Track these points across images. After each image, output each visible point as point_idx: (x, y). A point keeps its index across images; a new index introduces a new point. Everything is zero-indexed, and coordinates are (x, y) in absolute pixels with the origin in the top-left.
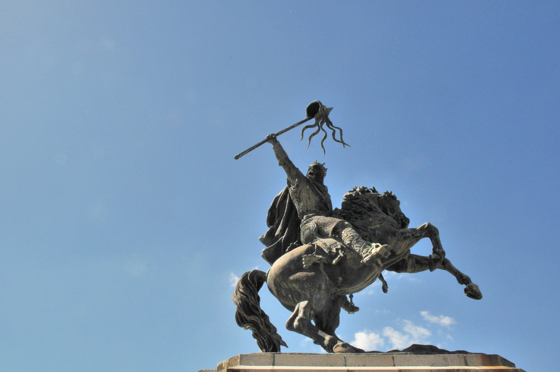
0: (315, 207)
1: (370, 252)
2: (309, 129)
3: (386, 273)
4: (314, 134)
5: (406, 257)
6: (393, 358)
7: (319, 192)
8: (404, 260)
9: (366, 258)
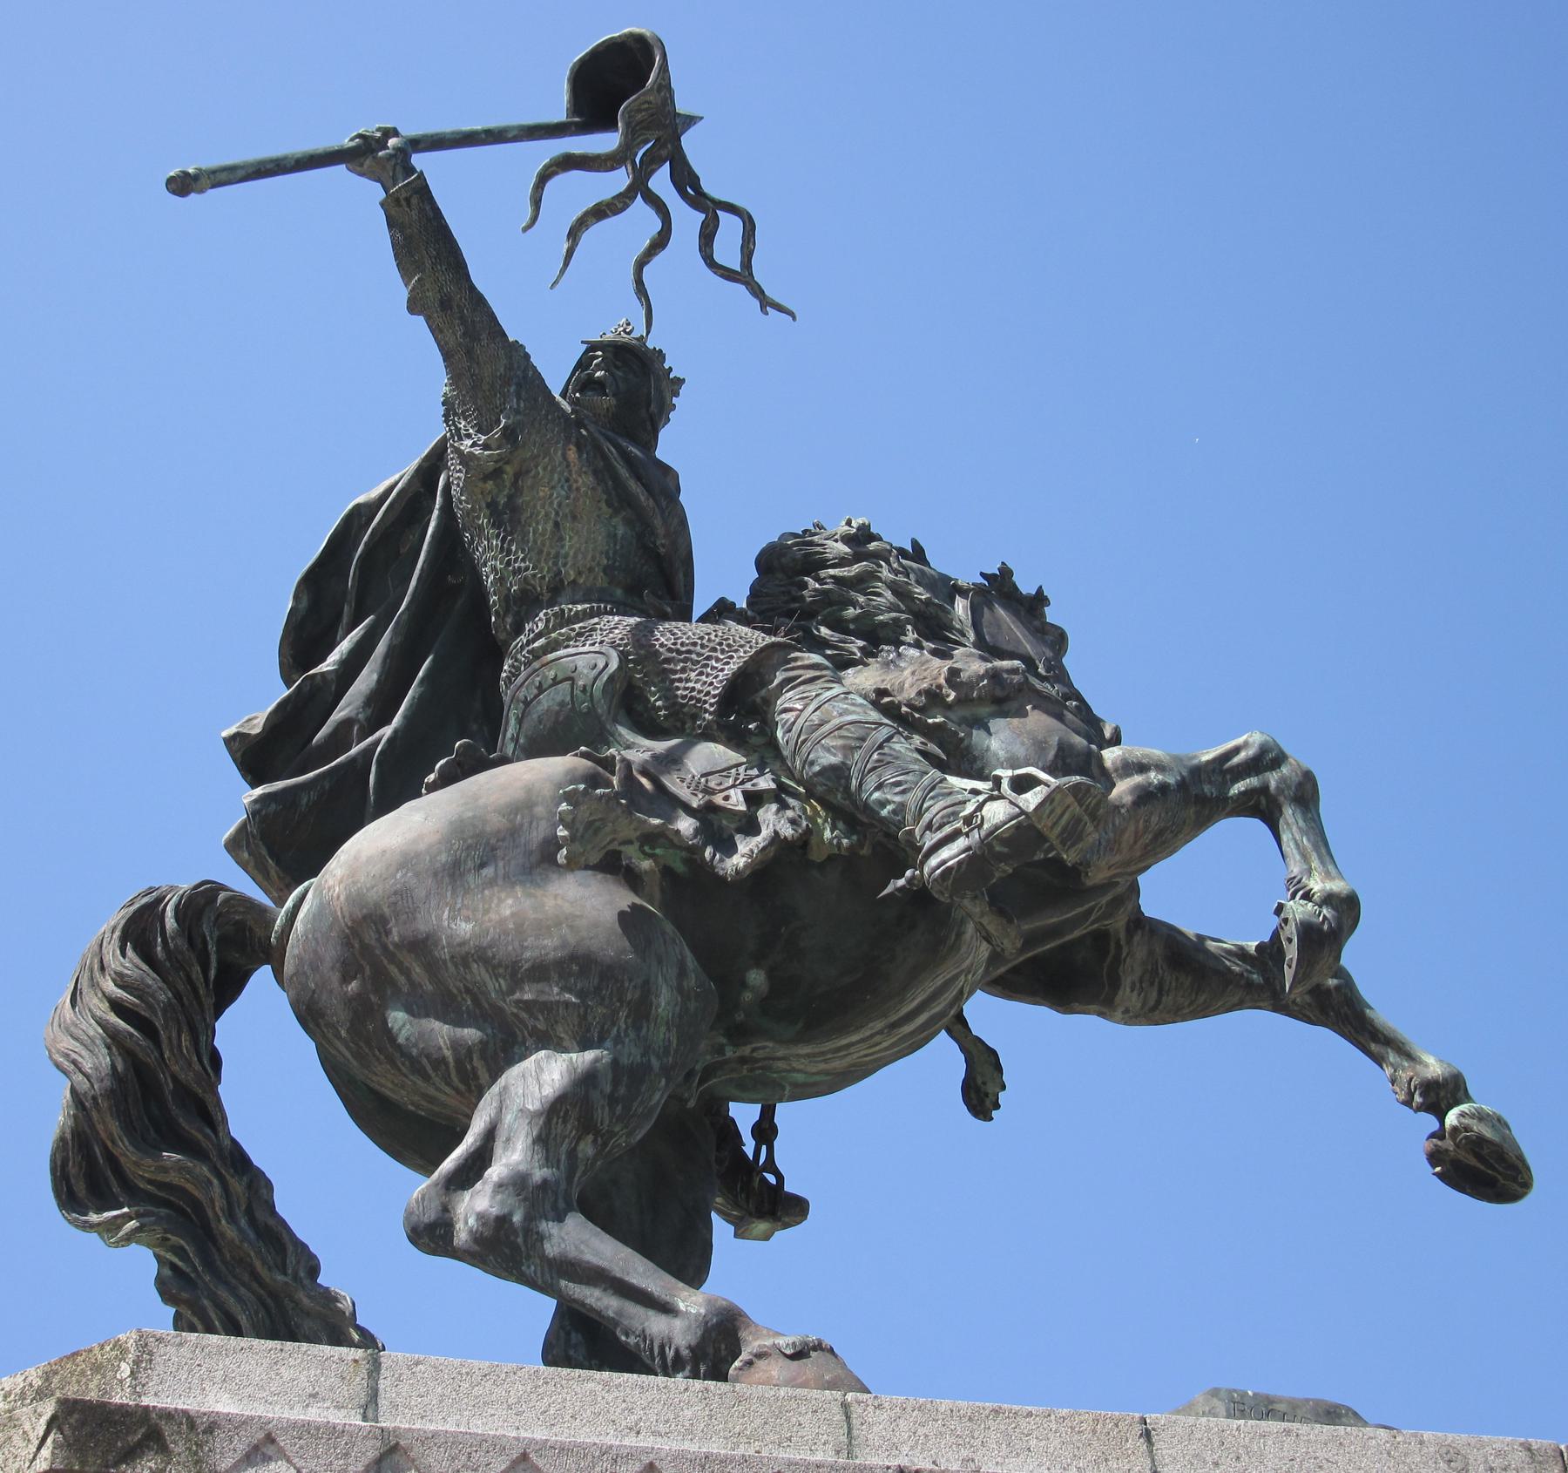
0: (607, 570)
1: (968, 821)
2: (575, 175)
3: (987, 1013)
4: (600, 212)
5: (1119, 923)
6: (1147, 1435)
7: (633, 485)
8: (1101, 939)
9: (945, 853)
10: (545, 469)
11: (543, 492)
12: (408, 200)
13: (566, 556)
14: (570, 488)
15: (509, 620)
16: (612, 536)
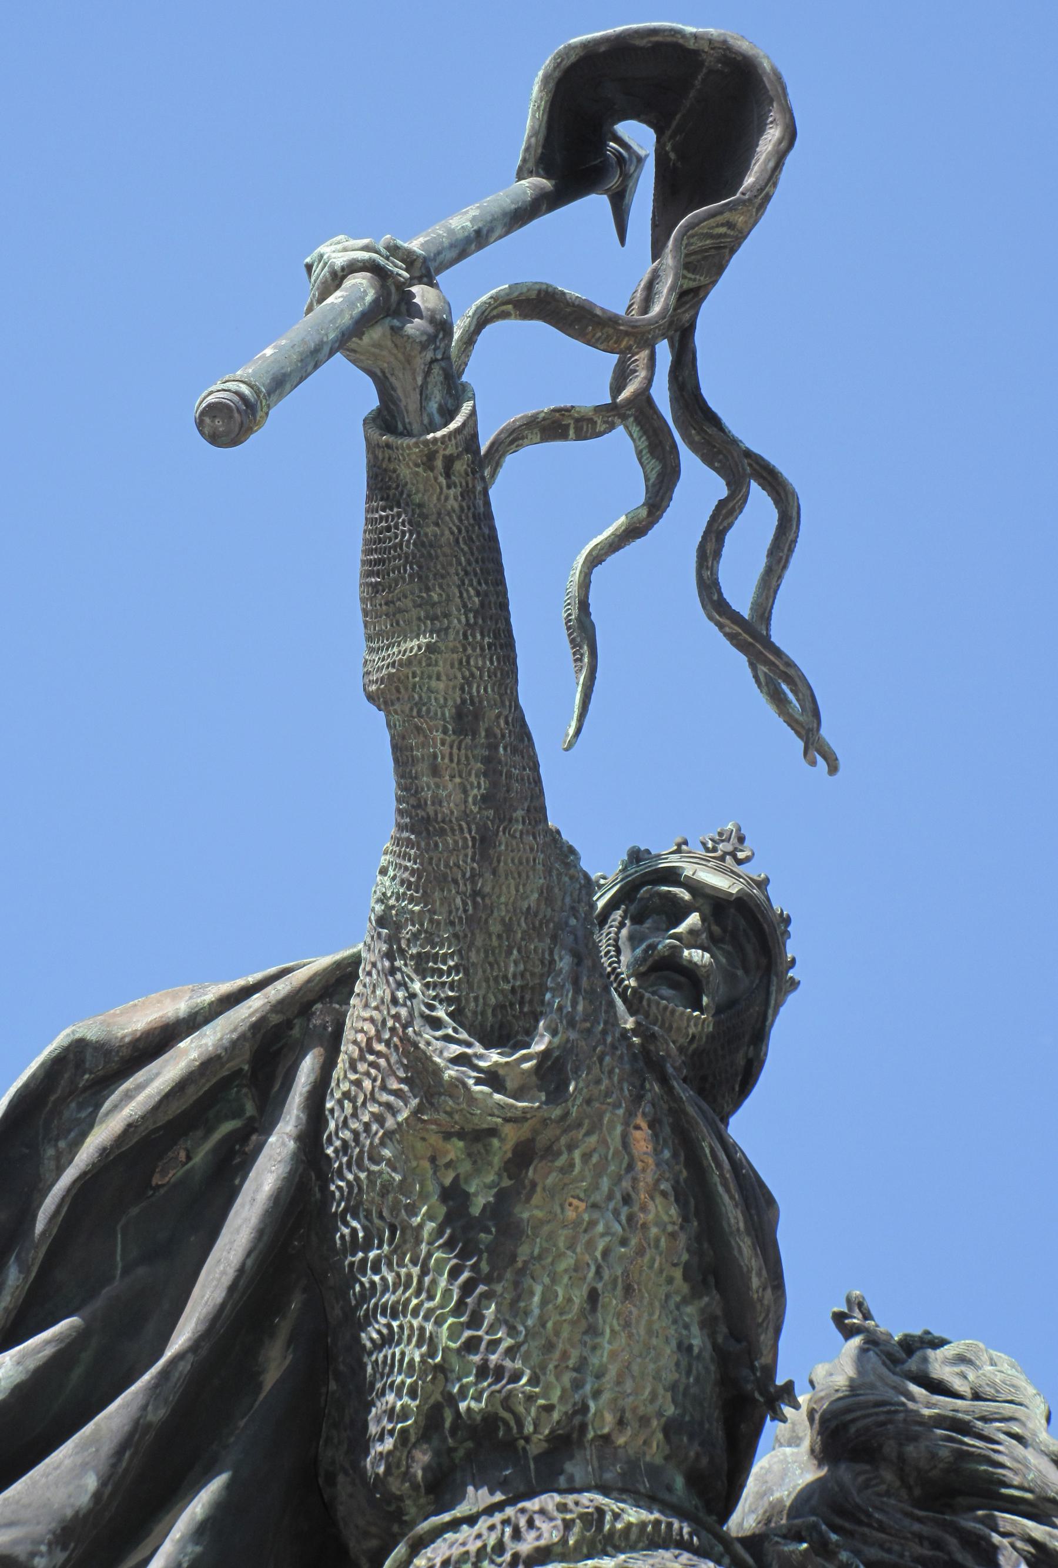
2: (539, 328)
10: (586, 1157)
11: (575, 1210)
12: (449, 461)
13: (599, 1376)
14: (631, 1218)
15: (422, 1458)
16: (684, 1348)
